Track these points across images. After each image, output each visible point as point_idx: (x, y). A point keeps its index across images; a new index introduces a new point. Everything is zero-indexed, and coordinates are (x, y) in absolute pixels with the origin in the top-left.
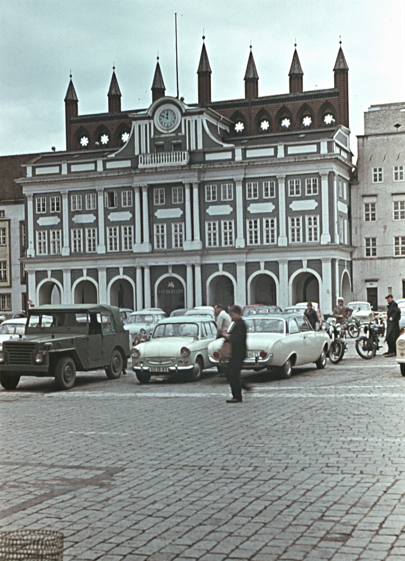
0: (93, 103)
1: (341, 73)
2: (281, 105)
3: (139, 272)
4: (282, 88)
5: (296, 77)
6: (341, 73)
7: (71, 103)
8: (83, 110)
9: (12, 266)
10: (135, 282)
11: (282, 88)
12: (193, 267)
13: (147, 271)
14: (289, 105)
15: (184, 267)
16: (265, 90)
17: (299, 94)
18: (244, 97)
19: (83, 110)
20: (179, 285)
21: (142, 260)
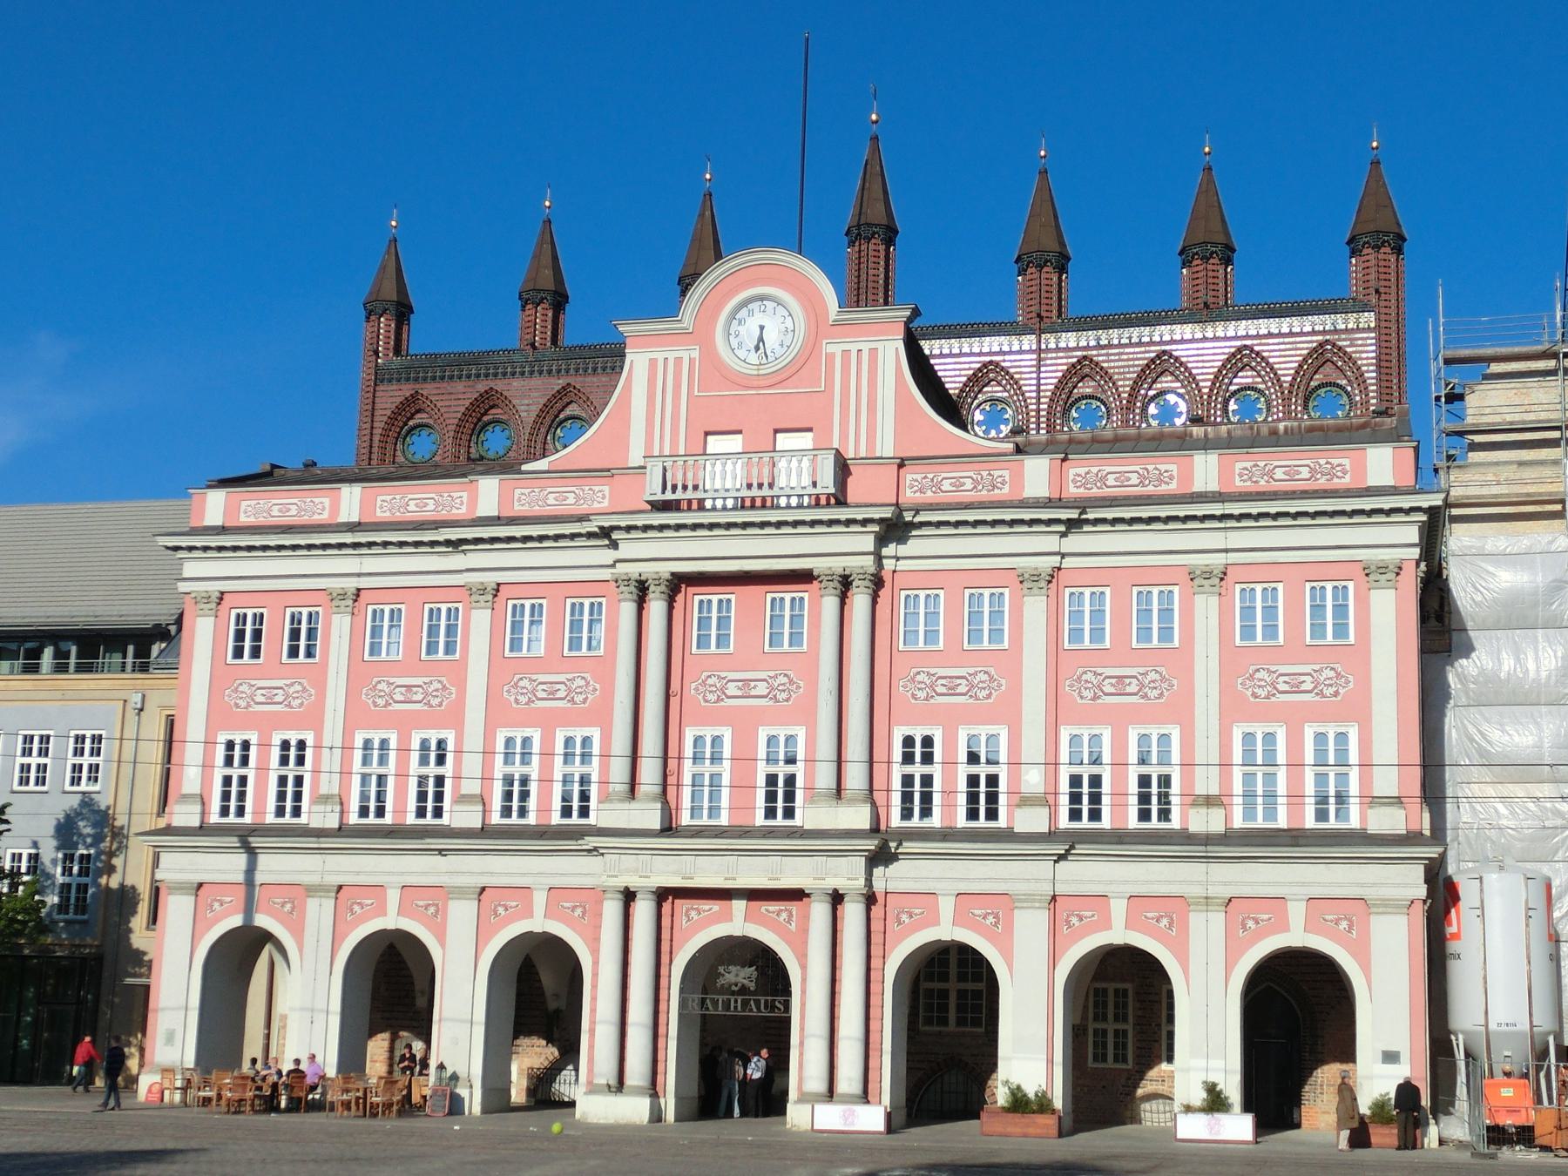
10: (595, 952)
13: (643, 911)
20: (772, 975)
21: (628, 861)
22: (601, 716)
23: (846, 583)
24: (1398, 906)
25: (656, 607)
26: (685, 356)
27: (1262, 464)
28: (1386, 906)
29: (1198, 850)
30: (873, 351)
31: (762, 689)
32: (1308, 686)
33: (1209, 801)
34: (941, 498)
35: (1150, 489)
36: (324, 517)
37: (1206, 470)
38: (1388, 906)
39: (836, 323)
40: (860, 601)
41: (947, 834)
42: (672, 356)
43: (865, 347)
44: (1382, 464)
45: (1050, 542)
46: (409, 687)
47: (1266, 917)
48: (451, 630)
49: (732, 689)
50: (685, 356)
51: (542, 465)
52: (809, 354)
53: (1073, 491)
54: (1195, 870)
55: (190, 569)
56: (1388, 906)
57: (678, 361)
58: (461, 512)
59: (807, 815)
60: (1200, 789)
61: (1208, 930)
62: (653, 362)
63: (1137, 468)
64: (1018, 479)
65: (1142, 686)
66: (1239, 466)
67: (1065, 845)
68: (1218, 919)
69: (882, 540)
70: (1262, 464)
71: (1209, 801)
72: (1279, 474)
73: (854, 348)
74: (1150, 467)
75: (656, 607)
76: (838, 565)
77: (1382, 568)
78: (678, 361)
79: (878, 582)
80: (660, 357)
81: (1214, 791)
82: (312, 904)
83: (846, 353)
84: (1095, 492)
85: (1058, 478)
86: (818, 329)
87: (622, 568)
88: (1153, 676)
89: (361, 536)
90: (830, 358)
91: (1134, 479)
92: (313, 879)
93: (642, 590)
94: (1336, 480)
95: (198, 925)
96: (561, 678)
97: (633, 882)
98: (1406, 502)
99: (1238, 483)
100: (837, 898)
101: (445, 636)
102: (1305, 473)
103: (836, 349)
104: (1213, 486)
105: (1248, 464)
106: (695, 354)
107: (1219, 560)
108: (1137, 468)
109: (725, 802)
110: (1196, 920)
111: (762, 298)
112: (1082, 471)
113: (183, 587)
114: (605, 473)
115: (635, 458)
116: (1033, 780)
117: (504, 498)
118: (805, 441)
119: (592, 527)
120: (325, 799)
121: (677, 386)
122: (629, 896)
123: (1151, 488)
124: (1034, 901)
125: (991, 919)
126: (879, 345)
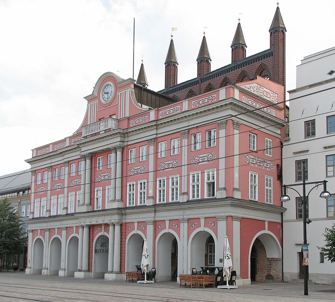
21: (83, 220)
24: (223, 218)
25: (88, 161)
27: (197, 101)
28: (221, 218)
32: (206, 160)
33: (184, 194)
45: (154, 132)
47: (196, 223)
54: (181, 212)
60: (183, 192)
61: (184, 227)
63: (172, 108)
66: (193, 102)
68: (186, 224)
70: (197, 101)
72: (201, 102)
74: (175, 107)
79: (123, 148)
80: (92, 104)
88: (175, 162)
90: (118, 95)
94: (213, 101)
95: (33, 238)
96: (78, 180)
97: (83, 224)
99: (192, 107)
103: (119, 94)
104: (187, 109)
105: (194, 102)
108: (172, 108)
110: (181, 225)
112: (162, 112)
121: (94, 110)
123: (175, 113)
124: (150, 223)
125: (144, 228)
126: (126, 90)
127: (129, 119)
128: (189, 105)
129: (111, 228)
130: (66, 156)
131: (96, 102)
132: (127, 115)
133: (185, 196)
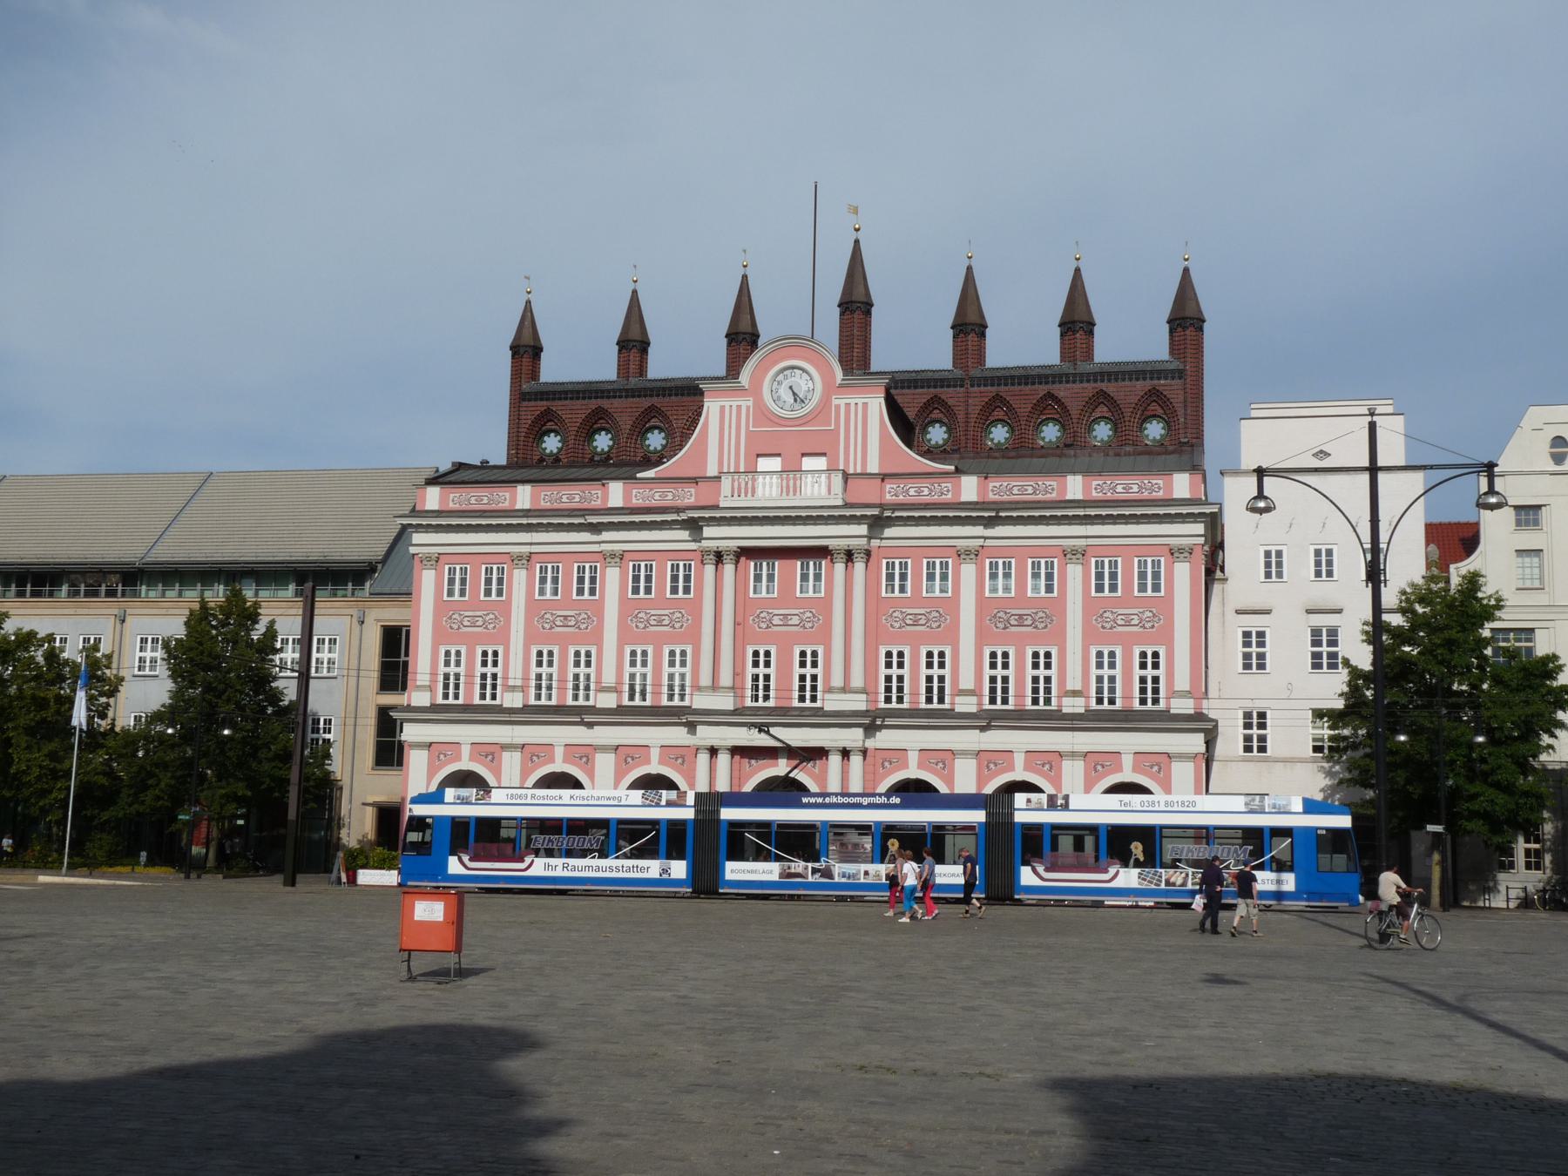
0: (580, 356)
1: (1186, 321)
2: (1042, 389)
3: (703, 758)
4: (1044, 350)
5: (1077, 324)
6: (1186, 321)
7: (526, 350)
8: (552, 370)
9: (1215, 766)
11: (1044, 350)
12: (845, 753)
13: (723, 759)
14: (1061, 391)
15: (819, 753)
16: (1001, 352)
17: (1084, 367)
18: (950, 367)
19: (552, 370)
22: (694, 637)
23: (849, 556)
25: (729, 569)
26: (744, 404)
29: (1067, 724)
30: (865, 404)
31: (795, 620)
32: (1135, 622)
33: (1075, 693)
34: (908, 500)
35: (1040, 497)
36: (506, 505)
37: (1074, 486)
38: (1182, 757)
39: (841, 386)
40: (859, 567)
41: (914, 713)
42: (734, 404)
43: (860, 401)
44: (1181, 485)
45: (979, 530)
46: (566, 617)
48: (593, 580)
49: (776, 621)
50: (744, 404)
51: (651, 473)
52: (825, 402)
53: (992, 497)
55: (417, 538)
56: (1182, 757)
57: (739, 407)
58: (597, 504)
59: (831, 703)
60: (1069, 687)
62: (723, 408)
64: (957, 490)
65: (1034, 620)
67: (986, 721)
69: (871, 527)
71: (1075, 693)
73: (853, 402)
75: (729, 569)
76: (843, 543)
77: (1181, 550)
78: (739, 407)
80: (727, 404)
81: (1078, 687)
82: (506, 755)
83: (848, 405)
84: (1005, 498)
85: (982, 489)
86: (830, 389)
87: (705, 543)
89: (533, 521)
90: (838, 407)
91: (1030, 490)
92: (508, 741)
93: (719, 557)
97: (716, 743)
98: (1196, 510)
100: (845, 753)
101: (590, 583)
102: (1135, 489)
103: (842, 402)
104: (1079, 497)
106: (750, 403)
107: (1083, 542)
109: (772, 693)
110: (1067, 765)
111: (793, 368)
113: (412, 550)
114: (695, 480)
115: (712, 471)
116: (967, 682)
117: (627, 496)
118: (821, 463)
119: (683, 516)
120: (513, 688)
122: (713, 751)
127: (884, 477)
128: (1086, 488)
129: (835, 760)
130: (606, 536)
131: (746, 403)
132: (873, 467)
133: (1080, 701)
